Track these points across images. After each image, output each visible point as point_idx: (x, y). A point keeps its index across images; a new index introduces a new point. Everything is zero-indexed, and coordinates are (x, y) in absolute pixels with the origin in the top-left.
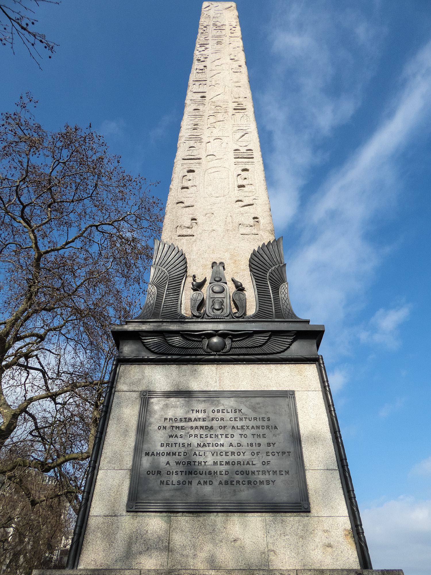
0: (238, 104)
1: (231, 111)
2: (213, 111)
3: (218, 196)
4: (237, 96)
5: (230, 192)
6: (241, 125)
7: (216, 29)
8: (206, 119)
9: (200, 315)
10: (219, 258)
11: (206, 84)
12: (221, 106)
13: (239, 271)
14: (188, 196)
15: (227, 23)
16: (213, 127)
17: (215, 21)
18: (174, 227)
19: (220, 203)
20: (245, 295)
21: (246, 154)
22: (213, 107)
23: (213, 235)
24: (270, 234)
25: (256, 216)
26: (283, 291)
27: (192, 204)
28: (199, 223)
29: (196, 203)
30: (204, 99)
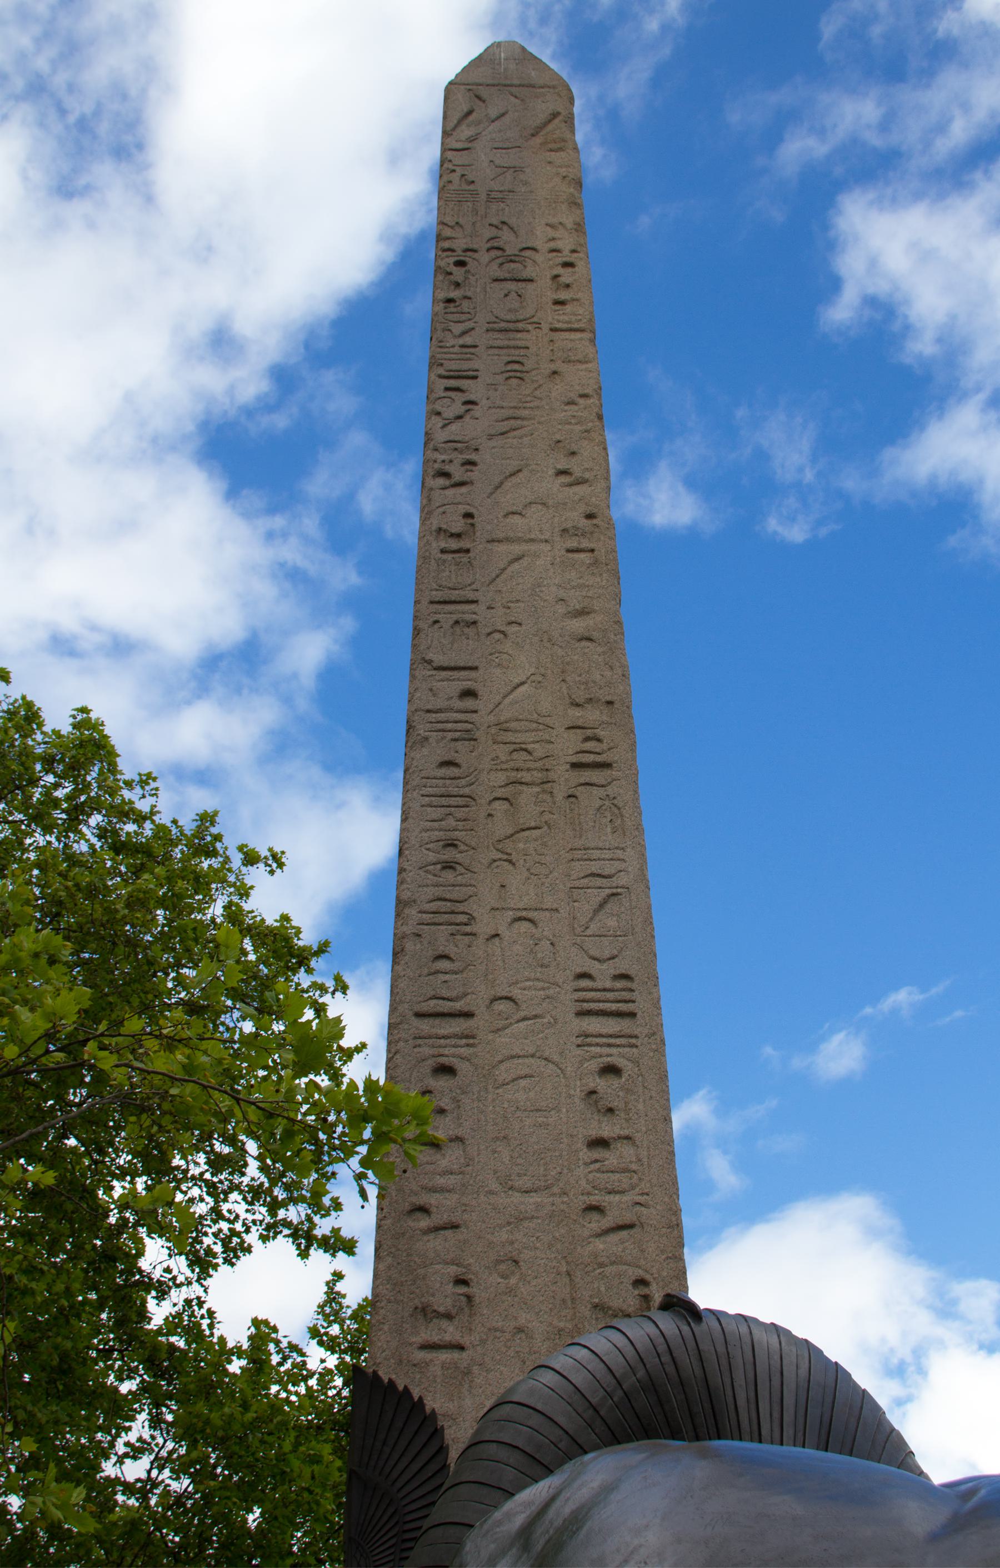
0: (587, 739)
1: (564, 778)
2: (501, 778)
3: (529, 1185)
4: (580, 696)
5: (565, 1171)
6: (596, 854)
7: (500, 274)
8: (483, 814)
11: (474, 623)
12: (530, 747)
14: (441, 1181)
15: (540, 238)
16: (505, 857)
17: (495, 222)
18: (407, 1314)
19: (537, 1218)
21: (610, 995)
22: (503, 755)
23: (517, 1349)
25: (640, 1273)
27: (455, 1219)
28: (477, 1300)
29: (466, 1216)
30: (469, 703)
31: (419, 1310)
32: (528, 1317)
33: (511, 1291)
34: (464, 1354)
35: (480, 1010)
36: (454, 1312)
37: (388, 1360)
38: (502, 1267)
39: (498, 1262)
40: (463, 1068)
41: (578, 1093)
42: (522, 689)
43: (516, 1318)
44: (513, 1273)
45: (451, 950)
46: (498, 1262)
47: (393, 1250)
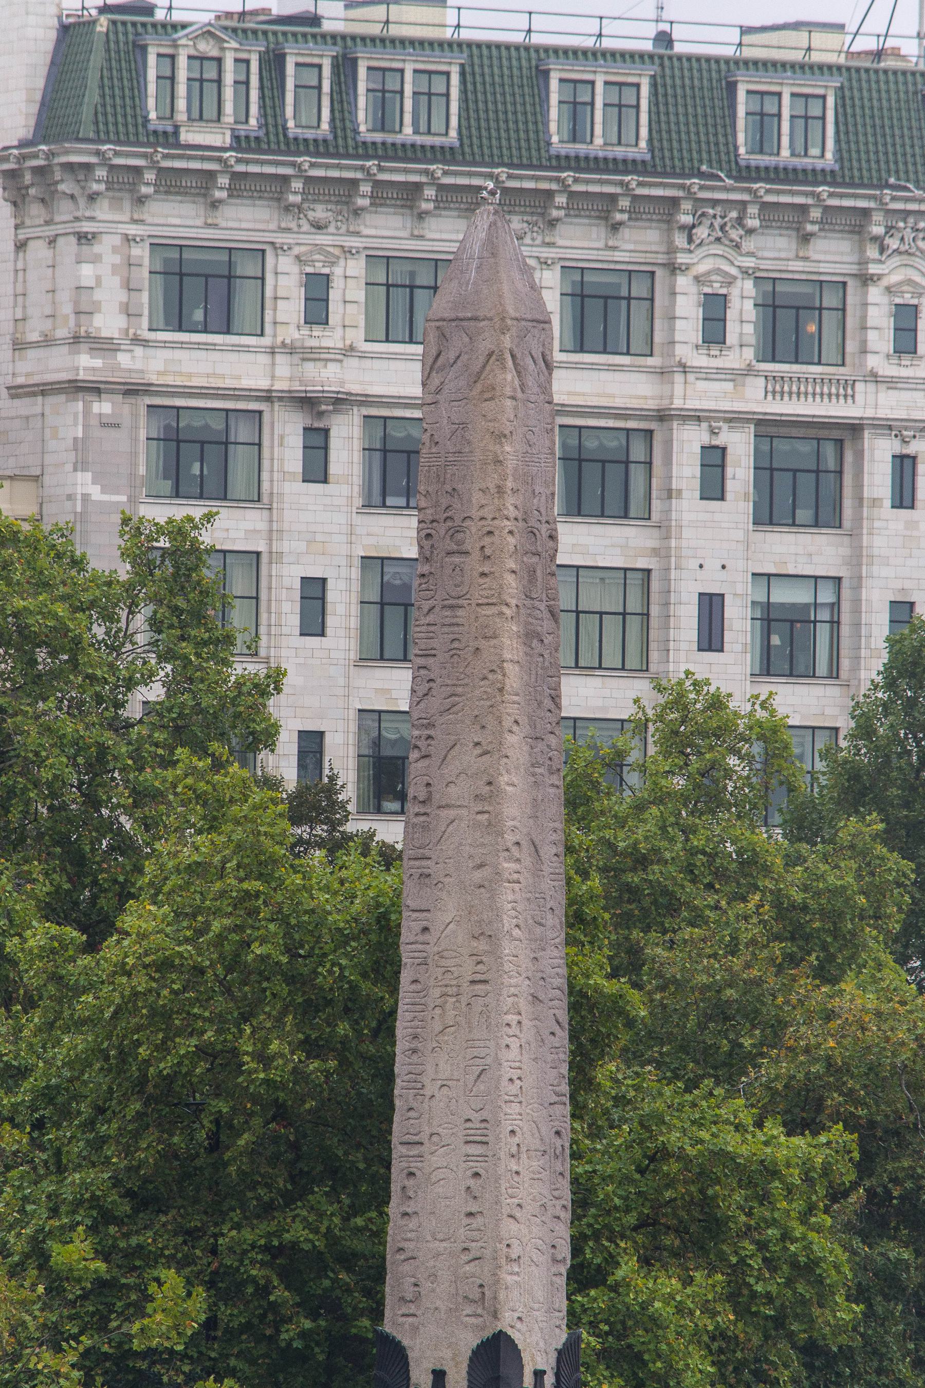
14: (409, 1235)
21: (479, 1132)
35: (426, 1141)
40: (418, 1173)
41: (463, 1188)
42: (451, 926)
45: (414, 1105)
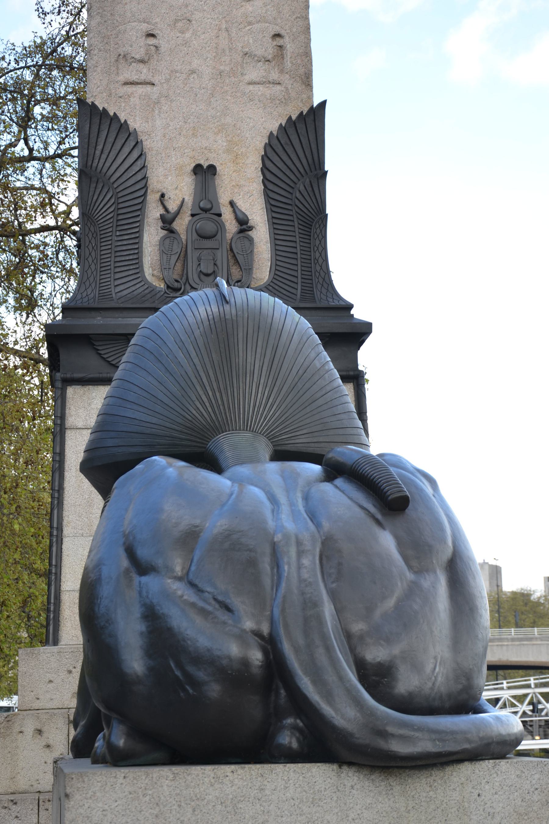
9: (179, 286)
10: (206, 148)
13: (242, 182)
18: (113, 60)
20: (251, 240)
24: (304, 87)
26: (318, 231)
28: (162, 50)
31: (121, 57)
32: (199, 62)
33: (186, 43)
34: (155, 88)
36: (146, 59)
37: (102, 93)
38: (180, 24)
39: (176, 21)
43: (190, 63)
44: (188, 29)
46: (176, 21)
47: (101, 11)
